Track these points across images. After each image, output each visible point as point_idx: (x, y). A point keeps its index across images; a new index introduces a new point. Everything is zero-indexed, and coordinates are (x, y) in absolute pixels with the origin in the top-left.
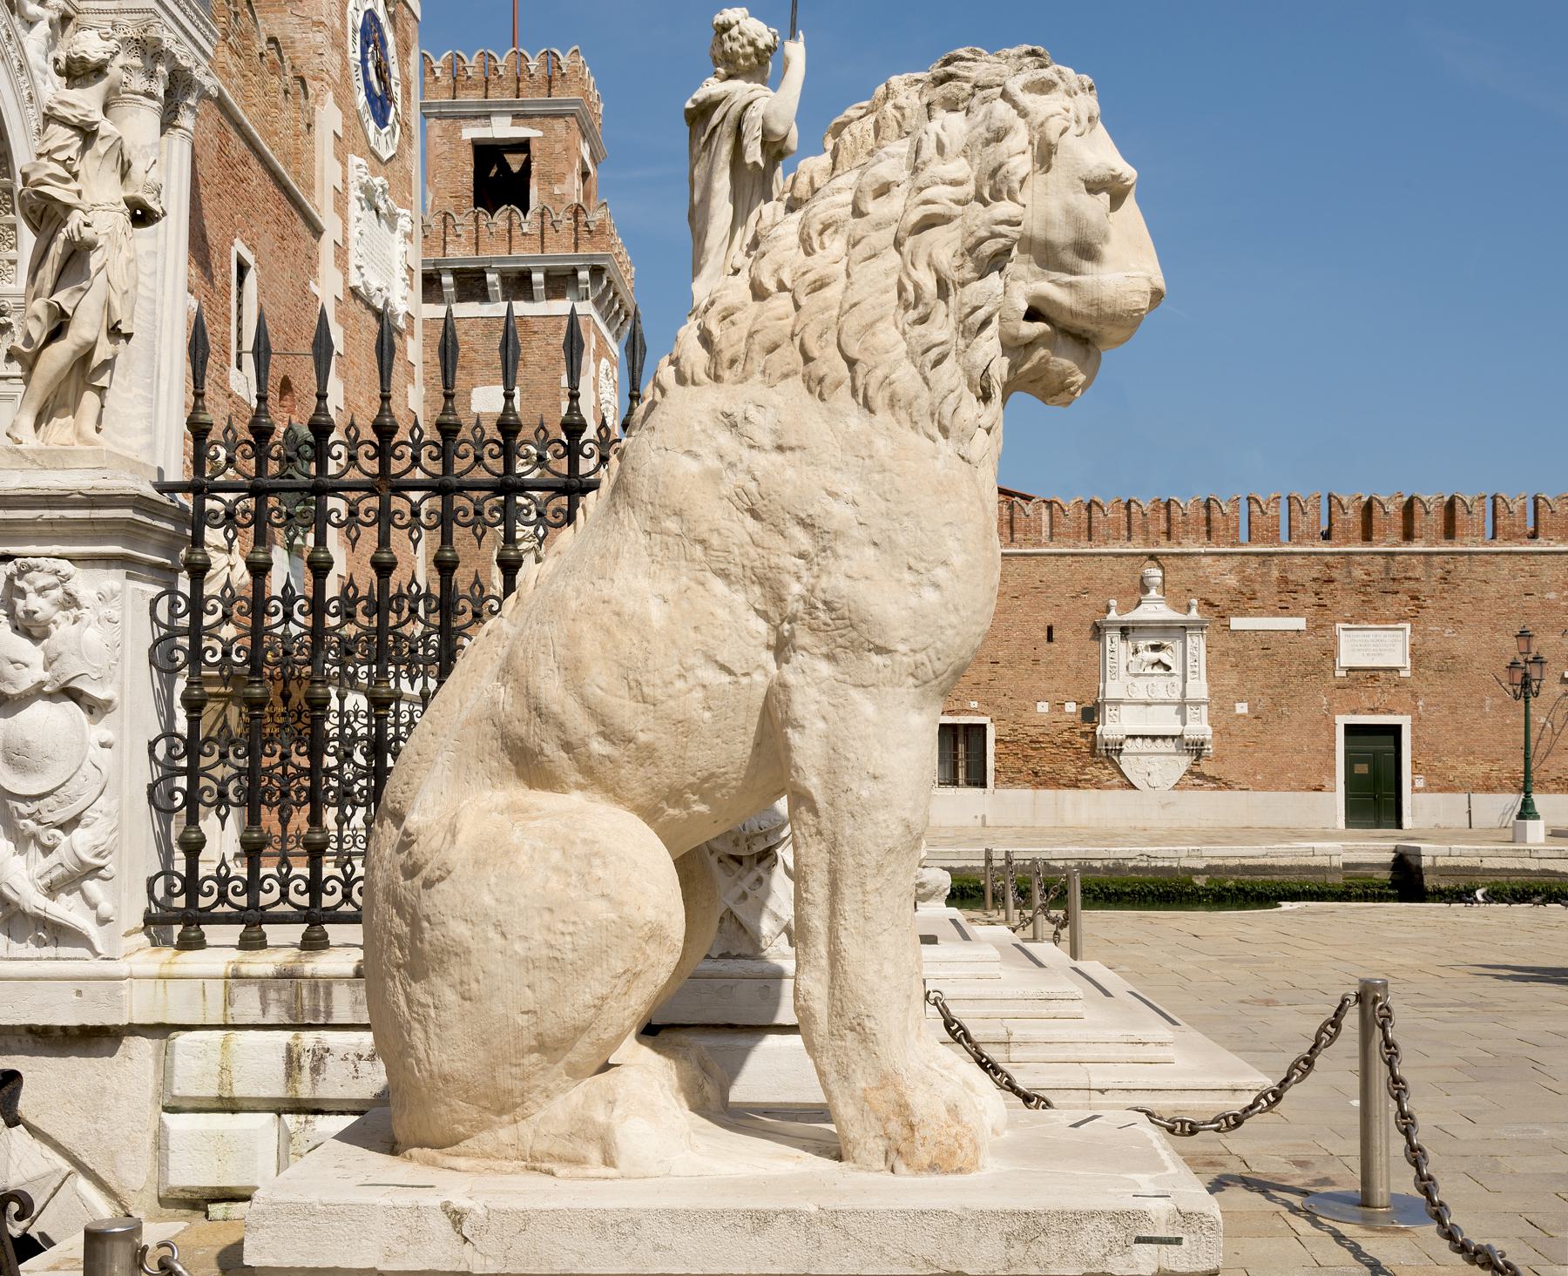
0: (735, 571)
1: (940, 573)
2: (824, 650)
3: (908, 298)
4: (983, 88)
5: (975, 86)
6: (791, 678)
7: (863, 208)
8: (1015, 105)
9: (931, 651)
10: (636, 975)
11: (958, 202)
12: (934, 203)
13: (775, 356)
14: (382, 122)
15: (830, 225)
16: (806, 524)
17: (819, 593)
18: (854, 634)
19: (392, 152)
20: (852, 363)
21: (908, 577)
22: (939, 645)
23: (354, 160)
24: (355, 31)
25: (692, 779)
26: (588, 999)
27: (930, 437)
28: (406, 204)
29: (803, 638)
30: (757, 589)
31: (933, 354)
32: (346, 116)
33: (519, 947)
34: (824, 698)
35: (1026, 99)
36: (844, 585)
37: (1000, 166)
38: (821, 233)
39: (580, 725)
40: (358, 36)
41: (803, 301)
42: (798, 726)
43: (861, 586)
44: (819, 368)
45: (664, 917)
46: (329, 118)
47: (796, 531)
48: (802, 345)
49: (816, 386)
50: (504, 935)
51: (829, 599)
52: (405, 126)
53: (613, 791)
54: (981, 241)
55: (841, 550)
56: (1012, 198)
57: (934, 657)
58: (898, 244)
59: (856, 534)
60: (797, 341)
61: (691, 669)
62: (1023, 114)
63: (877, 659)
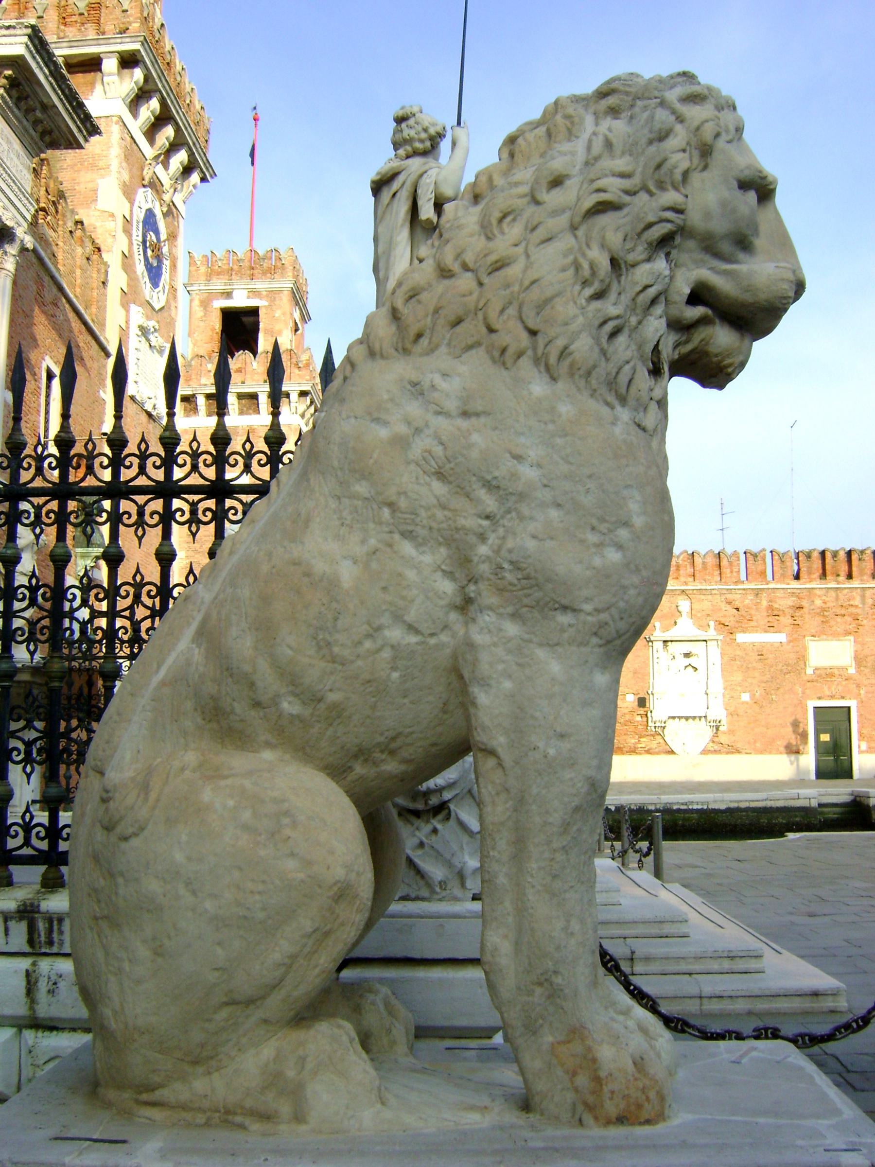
0: (422, 532)
1: (623, 534)
2: (510, 609)
6: (479, 638)
9: (613, 611)
10: (327, 934)
11: (627, 192)
12: (605, 191)
13: (458, 329)
15: (509, 213)
16: (491, 486)
17: (504, 553)
18: (539, 594)
20: (533, 333)
21: (592, 538)
22: (622, 604)
23: (134, 308)
24: (138, 222)
25: (381, 739)
26: (277, 956)
27: (607, 404)
29: (489, 598)
30: (443, 551)
31: (609, 327)
33: (208, 905)
34: (509, 657)
36: (531, 545)
37: (665, 160)
38: (501, 220)
39: (268, 680)
41: (486, 280)
42: (484, 683)
43: (549, 544)
44: (502, 339)
45: (353, 876)
46: (117, 279)
47: (482, 493)
48: (485, 319)
50: (194, 893)
51: (514, 559)
52: (173, 289)
53: (304, 752)
55: (525, 510)
56: (676, 189)
57: (617, 617)
58: (574, 228)
59: (540, 496)
60: (480, 315)
61: (379, 629)
63: (564, 619)
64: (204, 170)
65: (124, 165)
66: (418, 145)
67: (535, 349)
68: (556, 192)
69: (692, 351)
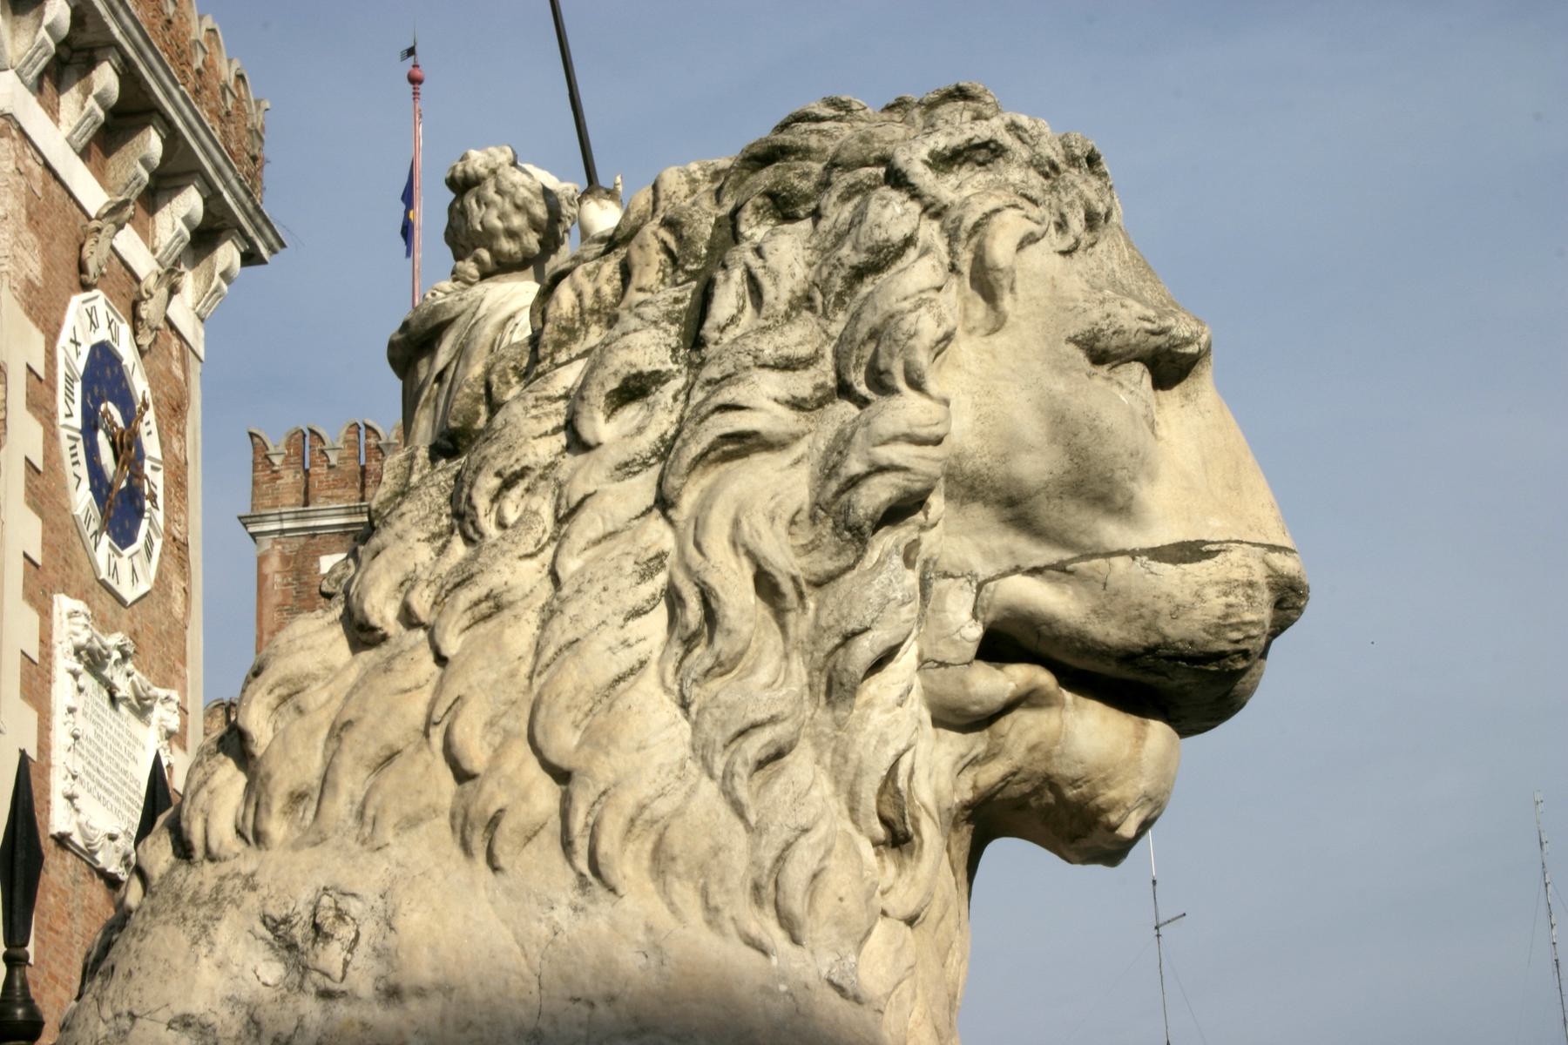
3: (696, 621)
4: (849, 167)
5: (833, 165)
7: (587, 434)
8: (915, 194)
11: (797, 404)
14: (124, 537)
19: (144, 586)
20: (562, 776)
23: (63, 604)
24: (70, 380)
28: (169, 674)
31: (755, 746)
32: (50, 527)
35: (945, 188)
38: (497, 497)
40: (78, 387)
44: (493, 795)
49: (479, 833)
52: (178, 548)
54: (854, 482)
56: (916, 384)
62: (935, 211)
64: (251, 232)
65: (28, 236)
66: (507, 246)
67: (565, 814)
68: (632, 414)
69: (1006, 780)
